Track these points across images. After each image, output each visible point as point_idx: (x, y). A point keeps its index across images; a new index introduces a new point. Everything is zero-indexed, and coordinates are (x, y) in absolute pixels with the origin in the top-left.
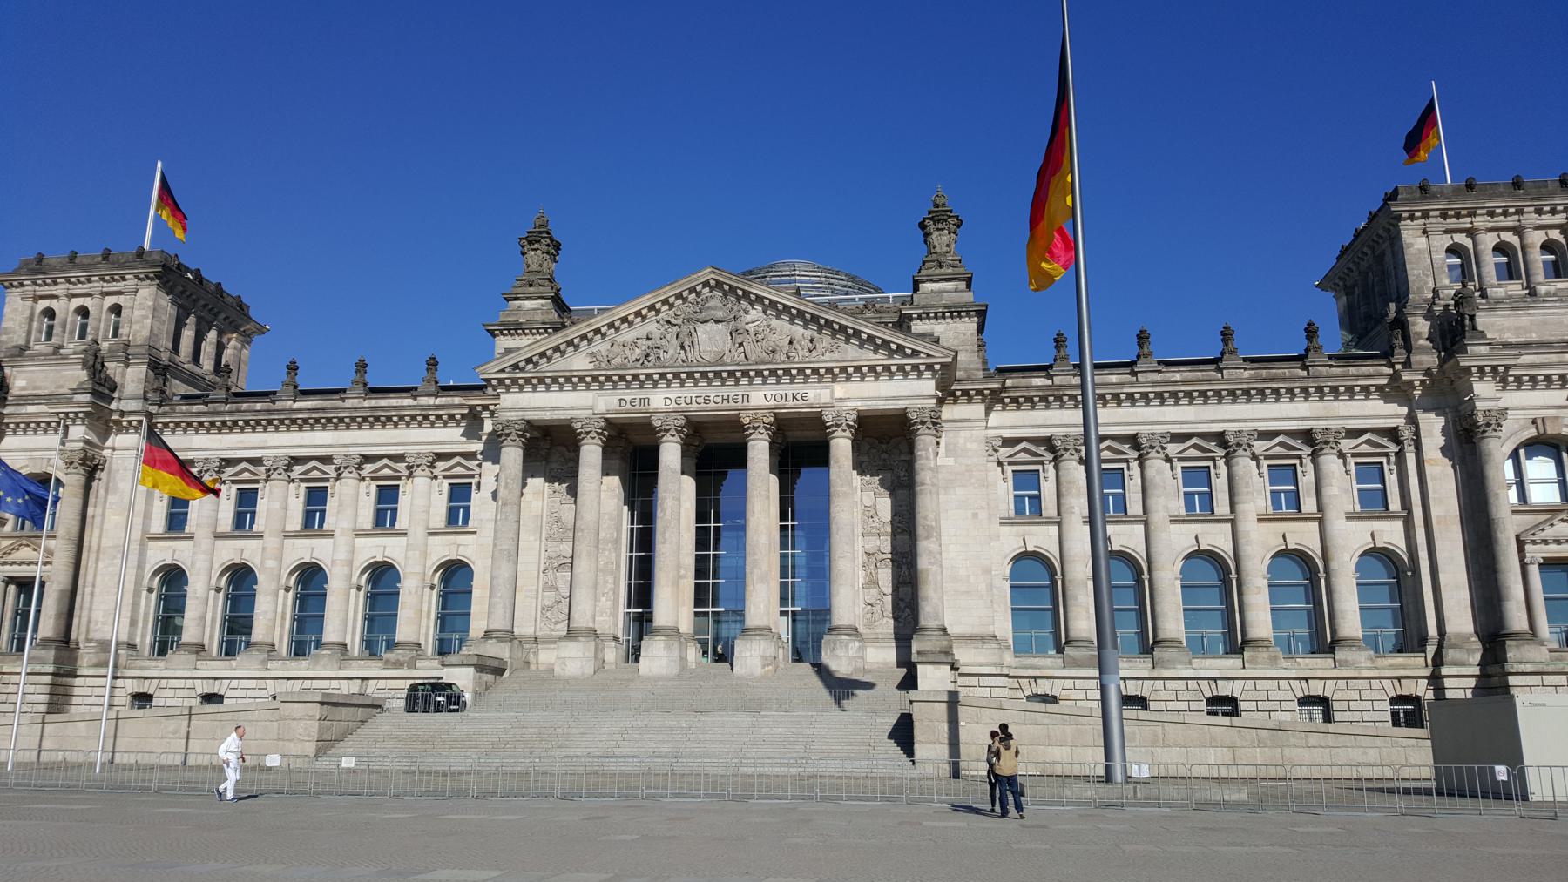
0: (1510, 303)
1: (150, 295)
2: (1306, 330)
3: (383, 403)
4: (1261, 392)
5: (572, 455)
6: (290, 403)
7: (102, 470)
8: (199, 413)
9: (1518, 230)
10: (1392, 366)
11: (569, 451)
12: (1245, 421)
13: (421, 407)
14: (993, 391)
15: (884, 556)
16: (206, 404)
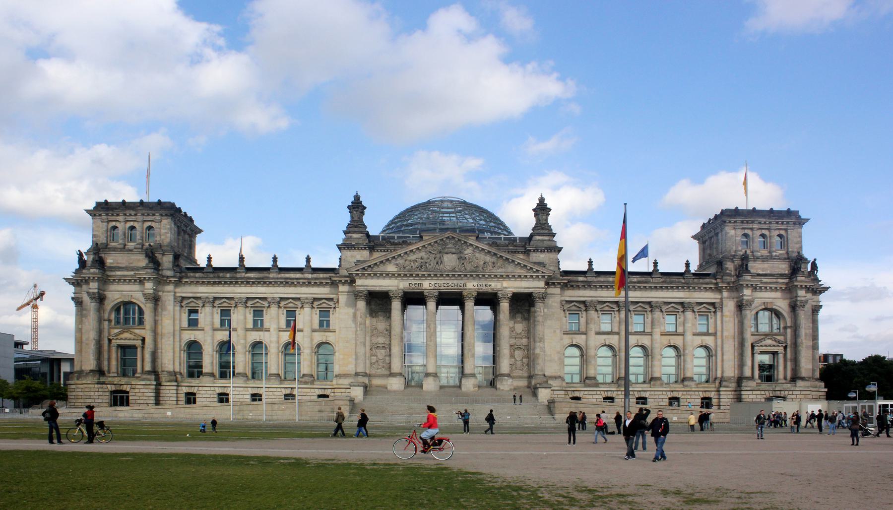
0: (761, 259)
1: (168, 223)
2: (685, 263)
3: (287, 275)
4: (667, 287)
5: (381, 302)
6: (244, 274)
7: (159, 301)
8: (200, 278)
9: (769, 229)
10: (716, 279)
11: (380, 301)
12: (659, 298)
13: (308, 279)
14: (564, 283)
15: (517, 347)
16: (203, 273)
